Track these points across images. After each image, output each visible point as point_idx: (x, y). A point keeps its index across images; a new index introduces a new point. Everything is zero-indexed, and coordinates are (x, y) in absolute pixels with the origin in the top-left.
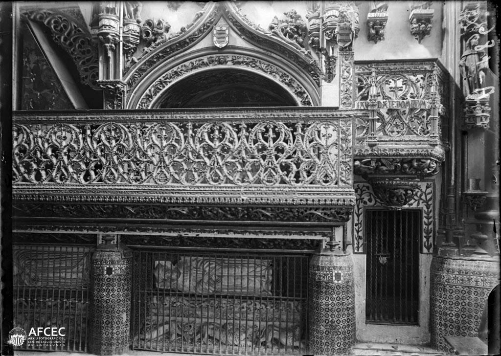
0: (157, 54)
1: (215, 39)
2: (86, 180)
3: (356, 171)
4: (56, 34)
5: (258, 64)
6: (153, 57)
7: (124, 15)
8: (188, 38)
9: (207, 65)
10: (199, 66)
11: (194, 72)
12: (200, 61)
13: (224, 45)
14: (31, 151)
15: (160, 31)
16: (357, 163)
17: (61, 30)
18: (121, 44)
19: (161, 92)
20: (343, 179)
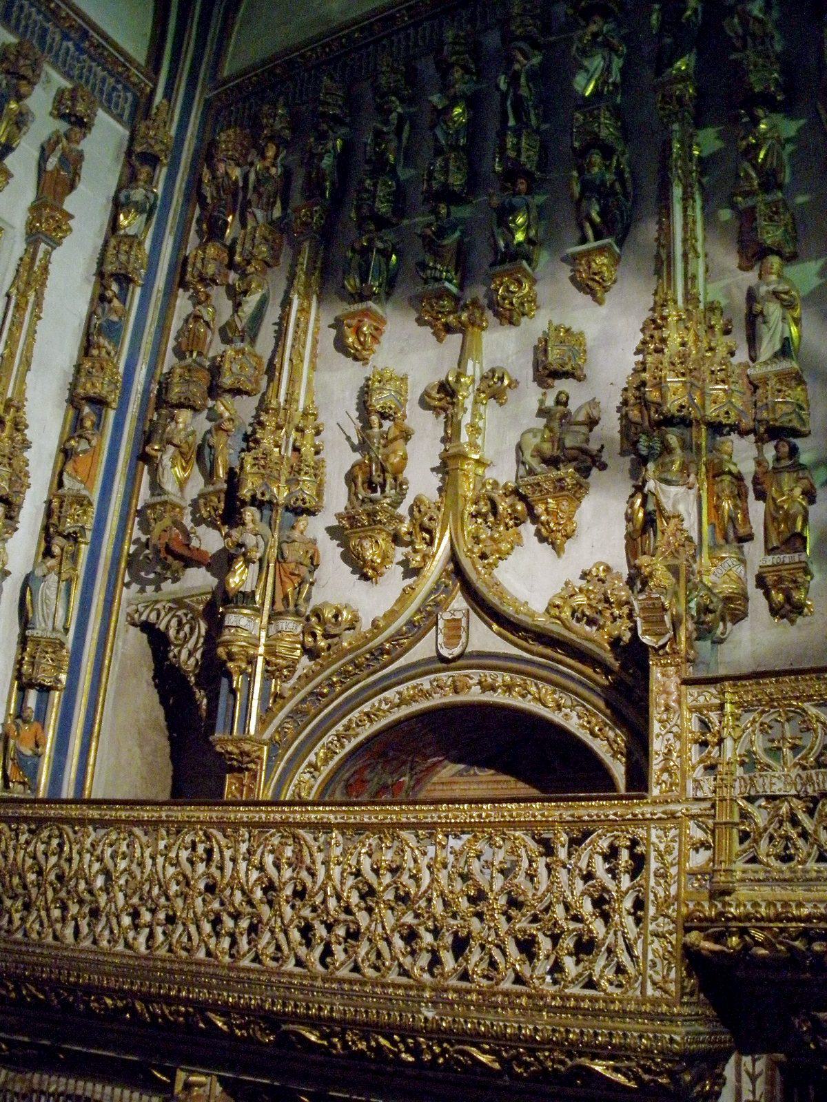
0: (329, 678)
1: (441, 639)
2: (148, 947)
3: (692, 958)
4: (176, 646)
5: (533, 689)
6: (320, 684)
7: (273, 603)
8: (387, 641)
9: (427, 695)
10: (413, 699)
11: (404, 711)
12: (414, 687)
13: (457, 651)
14: (71, 879)
15: (333, 631)
16: (694, 936)
17: (186, 640)
18: (260, 660)
19: (337, 758)
20: (658, 978)
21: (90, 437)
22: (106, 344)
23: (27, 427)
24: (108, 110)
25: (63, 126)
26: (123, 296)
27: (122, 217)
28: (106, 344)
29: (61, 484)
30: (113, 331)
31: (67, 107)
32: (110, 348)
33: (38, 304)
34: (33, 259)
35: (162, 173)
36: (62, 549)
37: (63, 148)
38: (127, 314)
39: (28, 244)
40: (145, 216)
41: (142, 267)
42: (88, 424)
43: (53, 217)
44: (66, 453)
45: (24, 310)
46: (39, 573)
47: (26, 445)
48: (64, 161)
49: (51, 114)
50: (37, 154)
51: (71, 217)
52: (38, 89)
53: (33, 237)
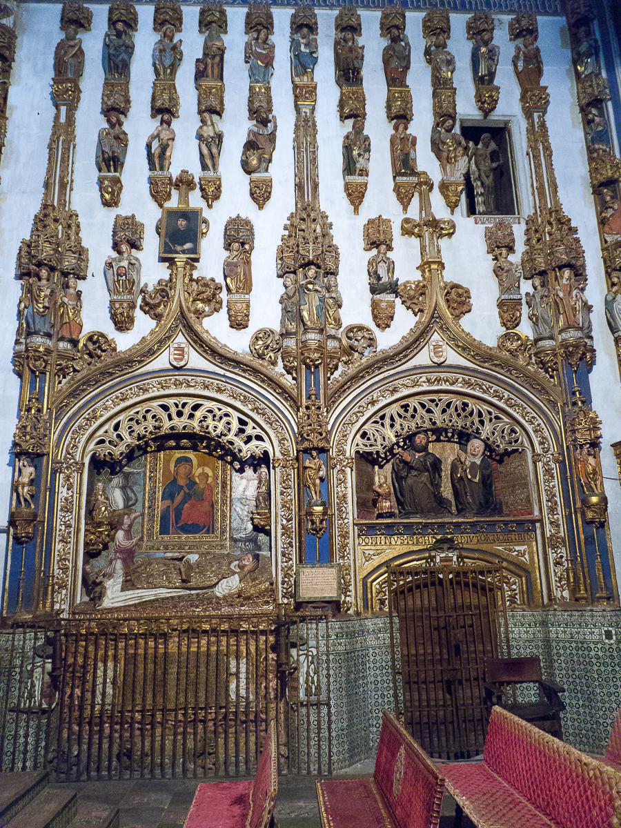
21: (611, 205)
22: (601, 146)
23: (570, 220)
24: (547, 14)
25: (520, 42)
26: (601, 115)
27: (579, 67)
28: (601, 146)
29: (606, 242)
30: (603, 137)
31: (517, 28)
32: (604, 148)
33: (547, 149)
34: (533, 126)
35: (595, 26)
36: (618, 278)
37: (524, 53)
38: (606, 123)
39: (528, 119)
40: (594, 57)
41: (605, 88)
42: (608, 198)
43: (533, 95)
44: (602, 222)
45: (539, 156)
46: (610, 298)
47: (573, 230)
48: (527, 59)
49: (511, 40)
50: (512, 68)
51: (546, 88)
52: (497, 34)
53: (528, 114)
